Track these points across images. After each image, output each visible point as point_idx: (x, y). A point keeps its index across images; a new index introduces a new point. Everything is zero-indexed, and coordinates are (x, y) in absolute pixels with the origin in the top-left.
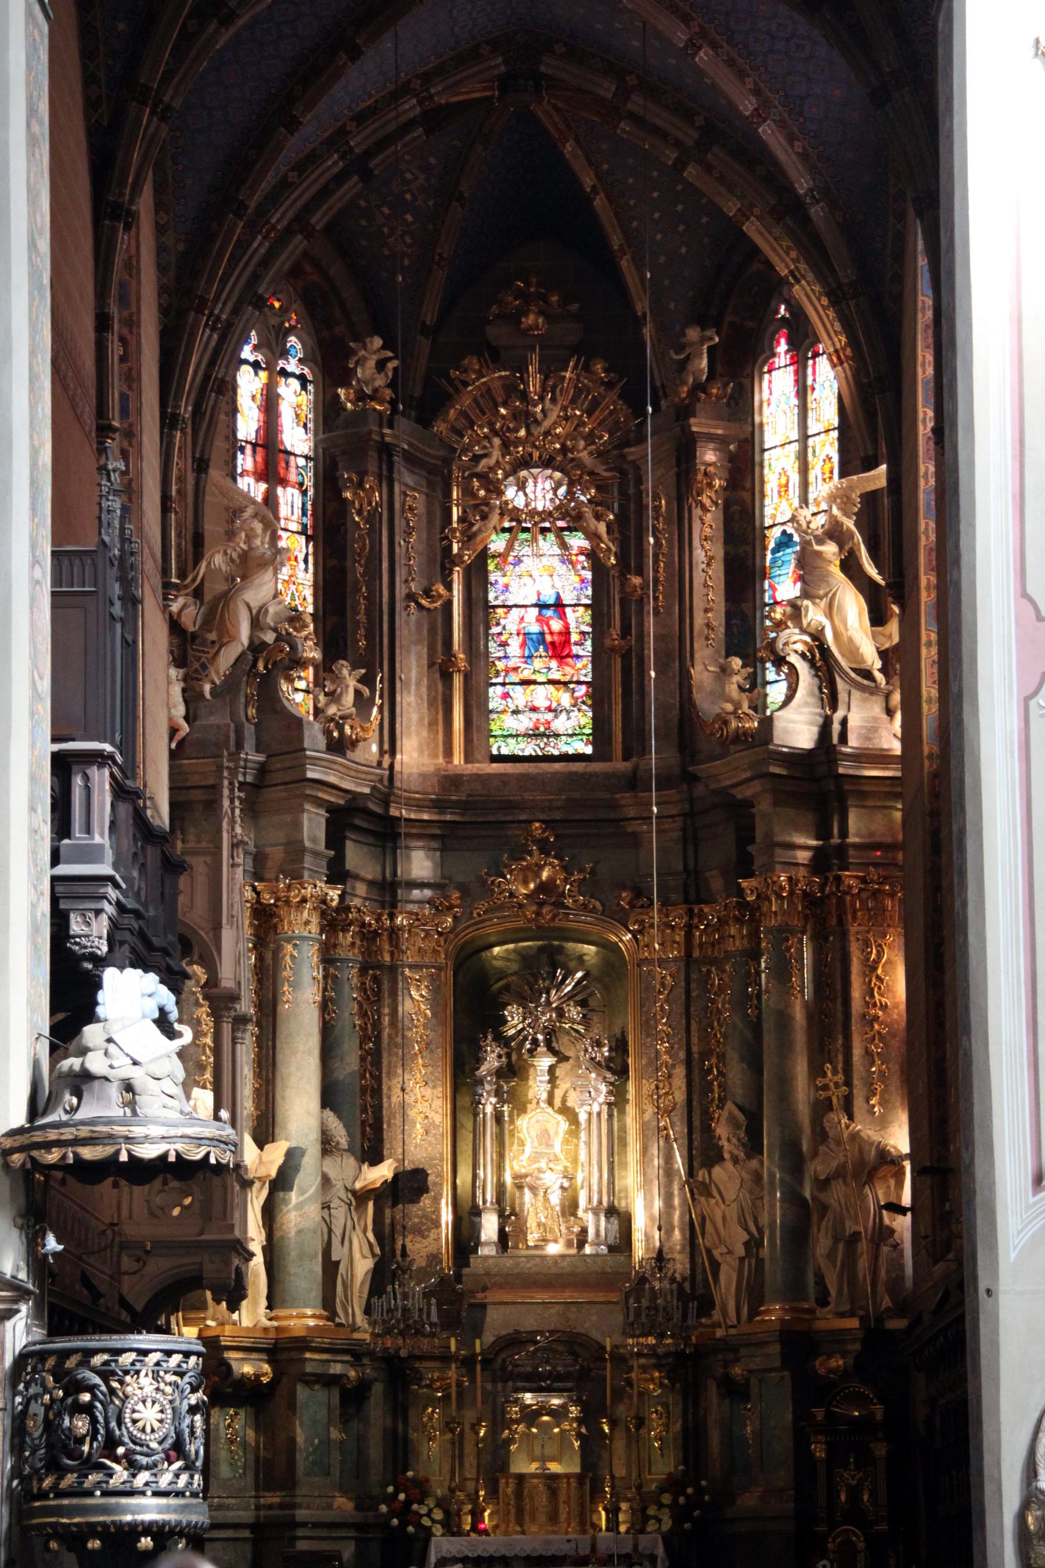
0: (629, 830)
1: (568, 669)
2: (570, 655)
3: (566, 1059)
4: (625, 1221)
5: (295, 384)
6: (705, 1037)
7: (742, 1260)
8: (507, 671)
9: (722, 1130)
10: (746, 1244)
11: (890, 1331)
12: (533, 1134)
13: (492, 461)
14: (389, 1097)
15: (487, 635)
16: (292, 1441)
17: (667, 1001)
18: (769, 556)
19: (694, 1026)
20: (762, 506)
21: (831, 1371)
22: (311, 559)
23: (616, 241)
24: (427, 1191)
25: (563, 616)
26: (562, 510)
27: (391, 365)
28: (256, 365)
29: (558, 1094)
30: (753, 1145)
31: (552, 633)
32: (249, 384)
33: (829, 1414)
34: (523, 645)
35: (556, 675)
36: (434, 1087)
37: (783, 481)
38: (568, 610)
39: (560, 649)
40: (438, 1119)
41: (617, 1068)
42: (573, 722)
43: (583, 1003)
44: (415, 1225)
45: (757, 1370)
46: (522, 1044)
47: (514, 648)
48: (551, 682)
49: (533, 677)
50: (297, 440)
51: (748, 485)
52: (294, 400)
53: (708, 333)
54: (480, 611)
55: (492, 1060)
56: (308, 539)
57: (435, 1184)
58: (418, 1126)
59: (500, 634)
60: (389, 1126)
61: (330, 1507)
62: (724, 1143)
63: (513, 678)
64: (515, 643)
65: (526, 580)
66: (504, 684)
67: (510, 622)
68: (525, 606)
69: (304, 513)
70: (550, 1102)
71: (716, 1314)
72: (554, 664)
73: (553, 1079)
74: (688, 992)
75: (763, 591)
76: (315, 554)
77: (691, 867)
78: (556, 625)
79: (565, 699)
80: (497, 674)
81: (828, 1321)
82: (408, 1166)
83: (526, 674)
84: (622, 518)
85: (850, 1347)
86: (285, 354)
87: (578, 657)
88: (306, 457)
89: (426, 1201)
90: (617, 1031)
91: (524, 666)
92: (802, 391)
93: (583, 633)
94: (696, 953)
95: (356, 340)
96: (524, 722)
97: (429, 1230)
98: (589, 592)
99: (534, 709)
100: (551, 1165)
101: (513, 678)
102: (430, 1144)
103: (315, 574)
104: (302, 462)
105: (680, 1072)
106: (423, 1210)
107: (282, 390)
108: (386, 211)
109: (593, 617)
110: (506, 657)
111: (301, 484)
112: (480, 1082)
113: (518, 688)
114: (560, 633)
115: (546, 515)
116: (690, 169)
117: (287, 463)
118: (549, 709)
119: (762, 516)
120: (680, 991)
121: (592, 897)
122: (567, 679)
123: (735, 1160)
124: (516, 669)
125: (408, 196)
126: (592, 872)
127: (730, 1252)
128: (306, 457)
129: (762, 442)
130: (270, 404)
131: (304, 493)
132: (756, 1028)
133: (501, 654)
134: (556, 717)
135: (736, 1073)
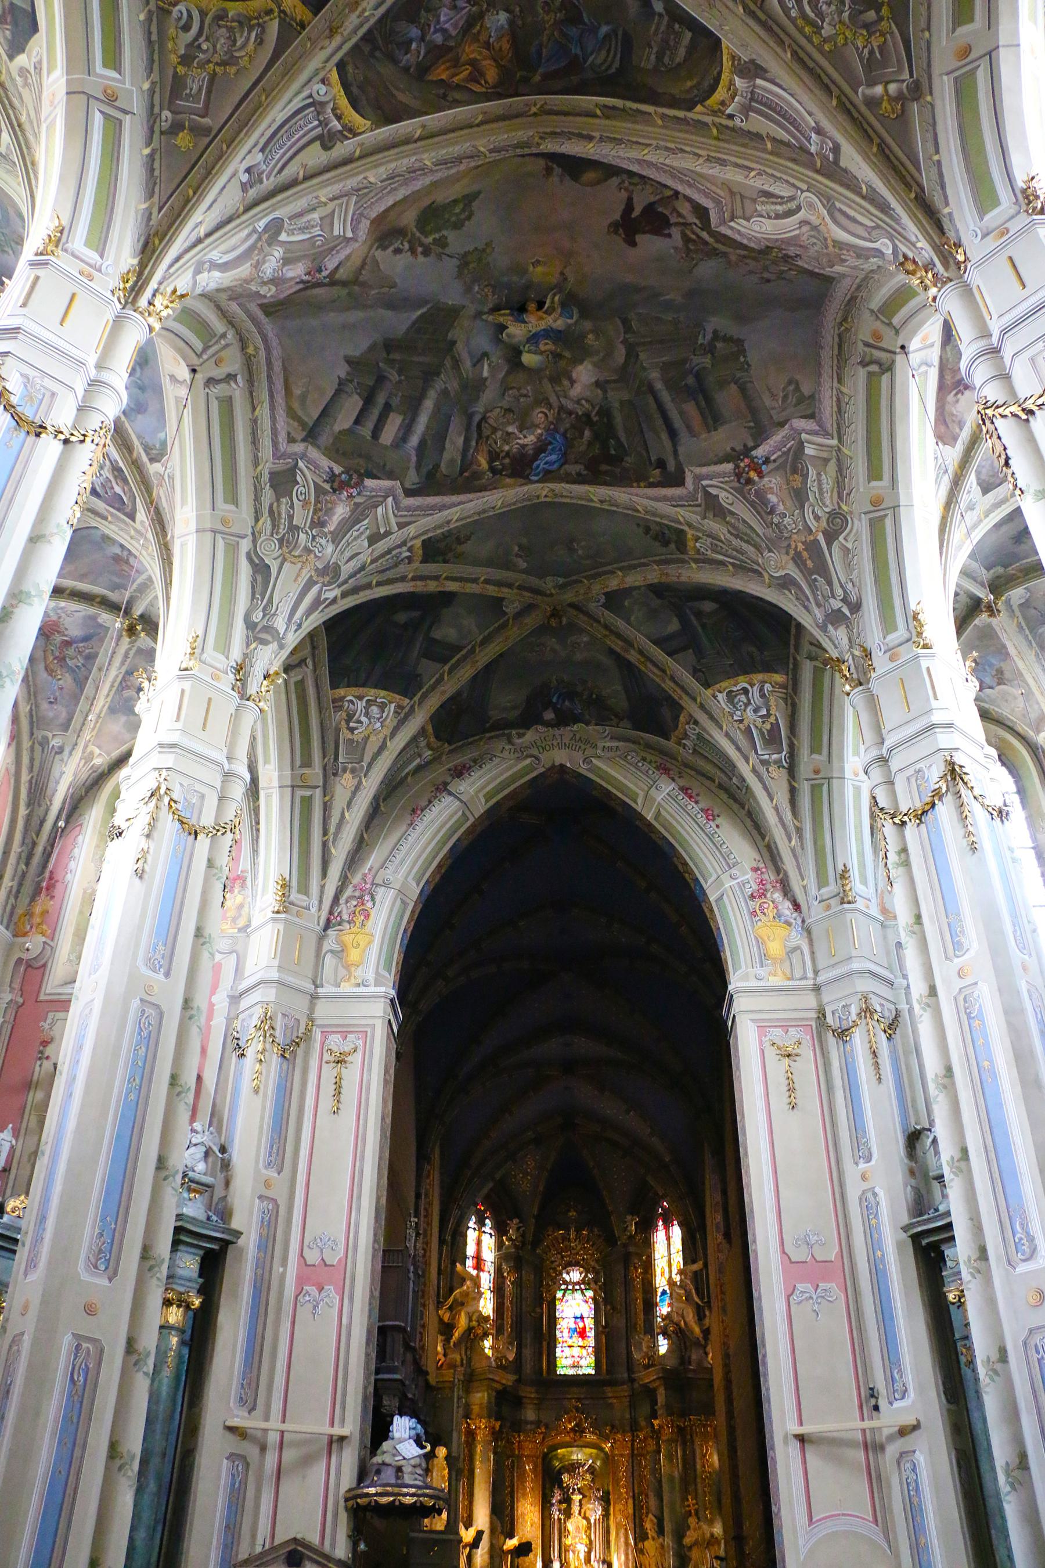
6: (639, 1486)
9: (648, 1525)
26: (583, 1282)
30: (661, 1531)
32: (472, 1236)
39: (582, 1334)
43: (592, 1473)
47: (566, 1334)
50: (489, 1255)
54: (553, 1320)
55: (557, 1496)
64: (566, 1332)
73: (581, 1505)
78: (581, 1325)
79: (584, 1352)
83: (570, 1342)
92: (668, 1238)
96: (570, 1362)
105: (630, 1501)
112: (553, 1505)
115: (578, 1283)
130: (479, 1243)
132: (660, 1482)
135: (653, 1502)
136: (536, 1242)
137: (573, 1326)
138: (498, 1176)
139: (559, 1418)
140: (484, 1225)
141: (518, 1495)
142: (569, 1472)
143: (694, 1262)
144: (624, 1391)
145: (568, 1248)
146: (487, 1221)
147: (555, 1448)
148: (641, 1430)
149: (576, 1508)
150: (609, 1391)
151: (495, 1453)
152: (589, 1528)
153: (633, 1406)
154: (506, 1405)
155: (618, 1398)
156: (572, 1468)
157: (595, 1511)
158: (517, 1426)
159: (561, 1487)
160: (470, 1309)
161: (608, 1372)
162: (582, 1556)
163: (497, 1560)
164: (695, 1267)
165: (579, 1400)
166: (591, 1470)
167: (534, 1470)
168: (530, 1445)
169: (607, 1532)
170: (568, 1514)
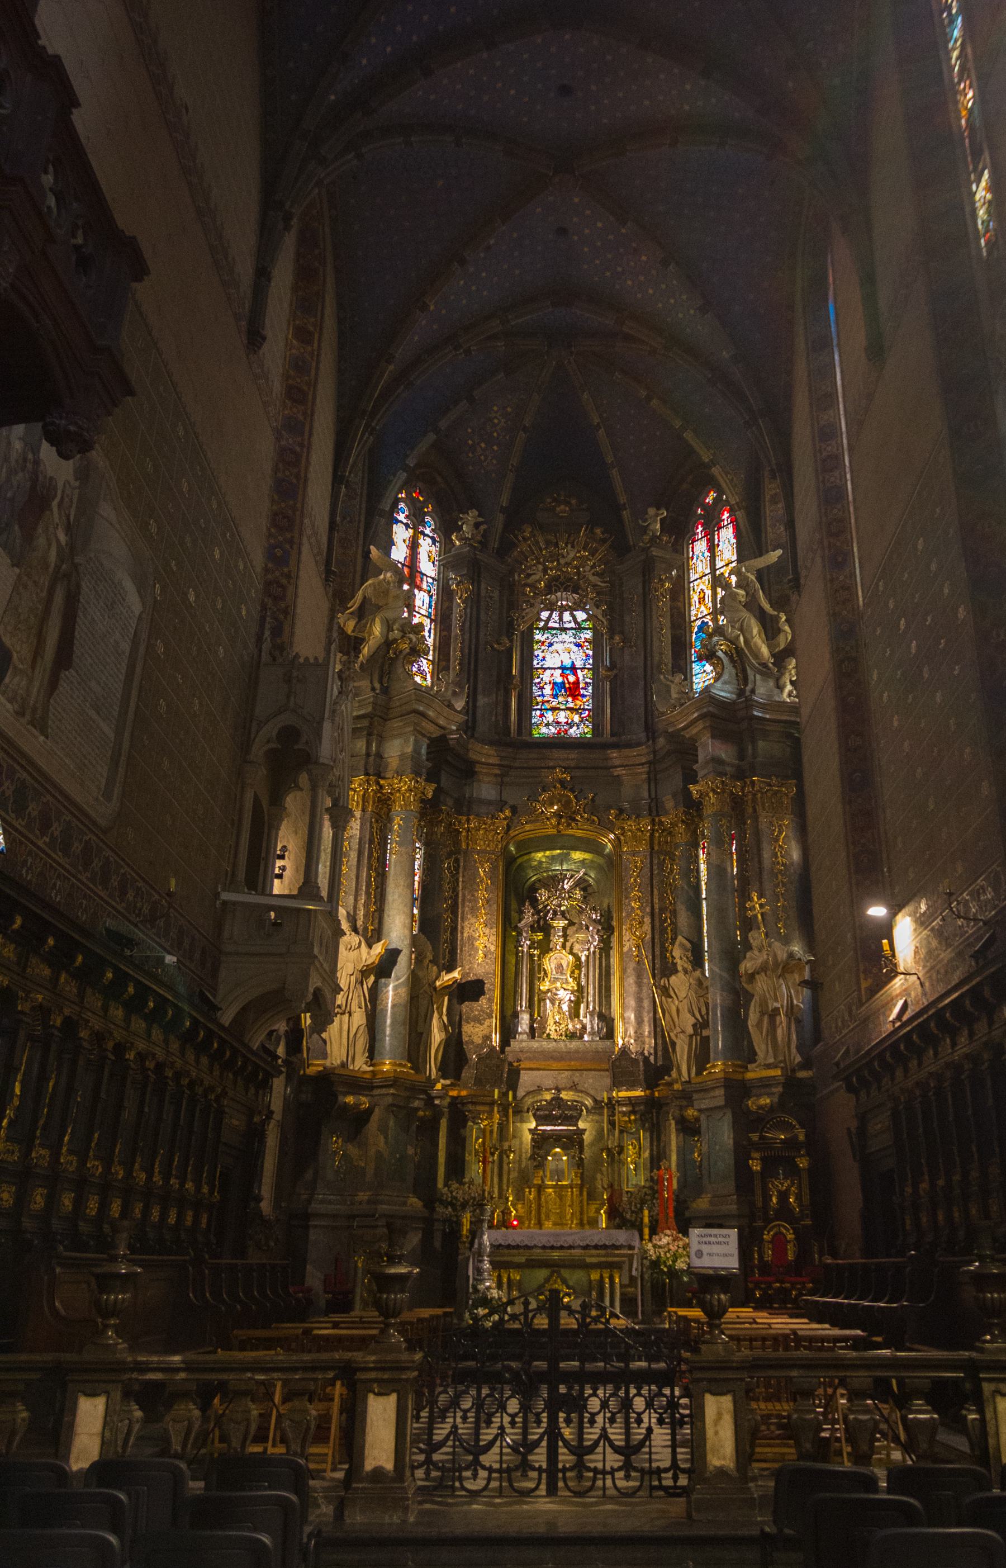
0: (616, 774)
1: (578, 702)
3: (574, 924)
4: (606, 1020)
5: (429, 541)
6: (662, 899)
7: (691, 1036)
8: (543, 702)
9: (677, 953)
10: (694, 1026)
11: (801, 1079)
12: (553, 966)
13: (537, 577)
14: (462, 933)
15: (532, 683)
17: (638, 876)
18: (694, 636)
19: (656, 892)
20: (690, 611)
21: (760, 1107)
23: (609, 459)
24: (483, 994)
25: (576, 674)
27: (483, 527)
28: (407, 526)
29: (568, 944)
31: (569, 683)
32: (401, 534)
33: (762, 1137)
34: (553, 689)
35: (571, 705)
36: (491, 928)
37: (702, 595)
38: (579, 671)
39: (574, 691)
40: (493, 948)
41: (607, 928)
42: (581, 730)
43: (584, 889)
44: (475, 1016)
45: (707, 1109)
46: (546, 915)
47: (548, 690)
51: (682, 600)
52: (428, 549)
53: (661, 512)
54: (528, 671)
55: (529, 917)
56: (432, 621)
57: (489, 990)
58: (480, 952)
59: (539, 683)
60: (461, 951)
62: (678, 961)
63: (547, 706)
65: (556, 654)
66: (541, 710)
67: (546, 676)
68: (554, 669)
69: (430, 606)
70: (564, 946)
71: (674, 1074)
72: (570, 699)
73: (565, 936)
74: (652, 871)
76: (435, 629)
77: (653, 796)
78: (572, 679)
81: (754, 1073)
82: (472, 977)
84: (611, 609)
85: (774, 1090)
86: (423, 523)
87: (584, 696)
88: (433, 578)
89: (483, 1001)
90: (605, 905)
93: (586, 683)
94: (656, 848)
95: (463, 513)
97: (484, 1019)
98: (591, 661)
99: (558, 723)
100: (564, 986)
101: (547, 706)
102: (487, 963)
103: (435, 640)
104: (430, 580)
105: (647, 920)
106: (481, 1006)
107: (421, 541)
108: (483, 445)
109: (593, 674)
110: (543, 695)
111: (429, 592)
113: (550, 713)
114: (574, 683)
116: (654, 401)
117: (422, 579)
118: (567, 723)
119: (690, 616)
120: (646, 871)
121: (592, 814)
123: (686, 972)
124: (548, 701)
125: (495, 434)
126: (593, 800)
127: (683, 1032)
128: (433, 578)
129: (689, 578)
130: (414, 546)
131: (431, 597)
134: (571, 727)
136: (505, 548)
137: (559, 680)
138: (443, 424)
139: (533, 797)
140: (423, 523)
141: (462, 910)
142: (547, 887)
143: (760, 552)
144: (640, 754)
145: (555, 557)
146: (428, 519)
147: (528, 846)
148: (666, 813)
149: (557, 940)
150: (614, 754)
151: (427, 844)
152: (578, 965)
153: (653, 779)
154: (445, 764)
155: (629, 767)
156: (553, 882)
157: (586, 943)
158: (465, 806)
159: (534, 902)
160: (390, 615)
161: (612, 735)
162: (565, 1007)
163: (424, 1003)
164: (761, 562)
165: (566, 769)
166: (582, 884)
167: (492, 874)
168: (483, 838)
169: (605, 975)
170: (545, 948)
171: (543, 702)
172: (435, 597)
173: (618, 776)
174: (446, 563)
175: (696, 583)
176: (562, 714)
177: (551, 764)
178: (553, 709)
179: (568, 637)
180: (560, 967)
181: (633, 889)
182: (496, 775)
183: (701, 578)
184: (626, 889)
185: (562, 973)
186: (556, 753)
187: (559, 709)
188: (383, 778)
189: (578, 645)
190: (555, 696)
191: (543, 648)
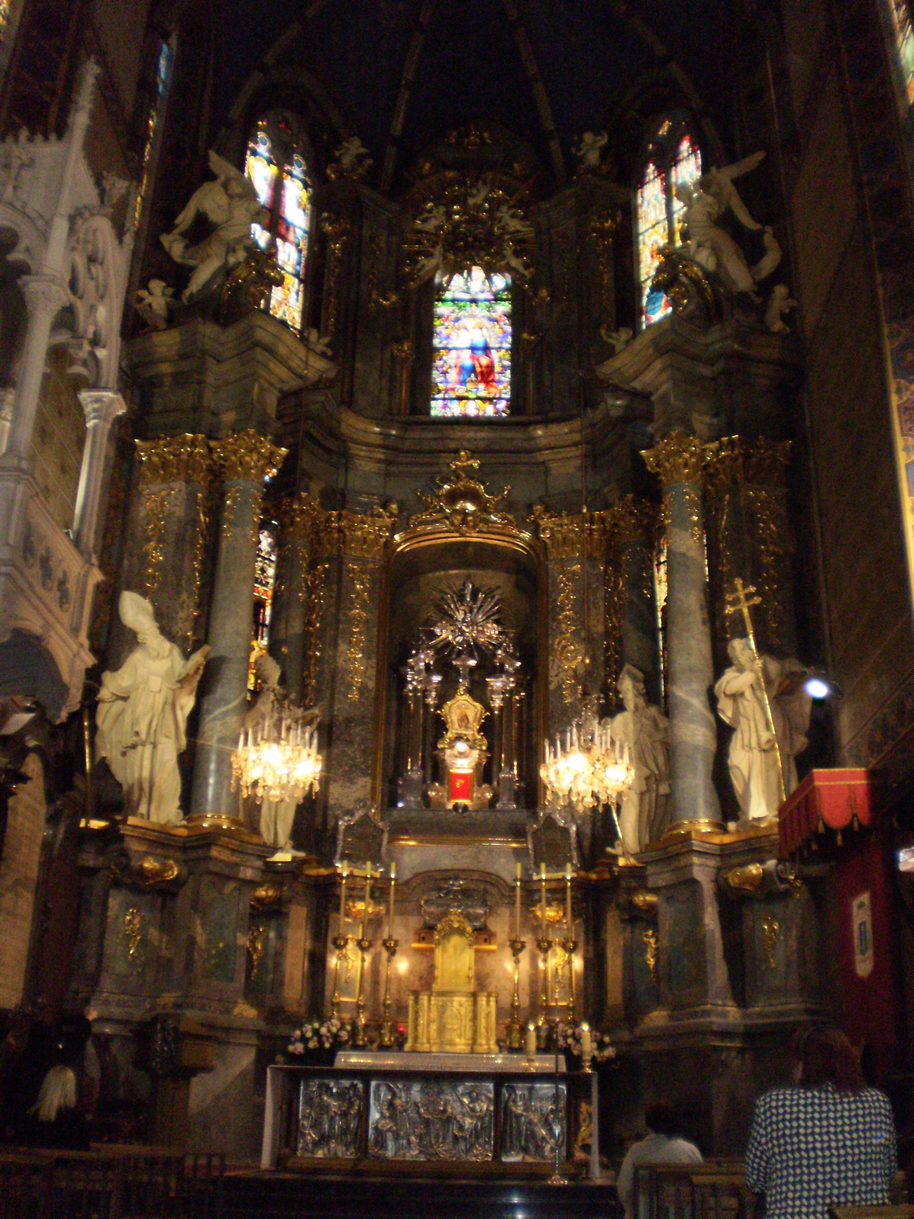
0: (541, 459)
1: (492, 389)
2: (493, 381)
8: (446, 391)
16: (192, 940)
18: (645, 300)
22: (301, 294)
31: (481, 366)
34: (459, 373)
35: (483, 394)
38: (493, 352)
39: (486, 375)
47: (453, 375)
48: (479, 398)
49: (466, 394)
56: (301, 281)
61: (228, 1011)
66: (444, 399)
67: (450, 358)
68: (462, 349)
72: (482, 386)
75: (640, 323)
78: (484, 361)
80: (439, 392)
83: (461, 391)
87: (500, 382)
91: (458, 386)
110: (446, 382)
113: (456, 402)
114: (487, 367)
122: (492, 396)
124: (453, 389)
131: (300, 251)
133: (442, 379)
137: (468, 363)
165: (474, 453)
171: (446, 391)
172: (305, 253)
173: (543, 463)
174: (320, 203)
175: (647, 234)
176: (471, 403)
177: (452, 445)
178: (460, 398)
179: (480, 311)
180: (464, 719)
181: (563, 610)
182: (379, 461)
183: (653, 227)
184: (553, 608)
185: (467, 727)
186: (457, 433)
187: (467, 398)
188: (217, 439)
189: (492, 320)
190: (463, 383)
191: (446, 323)
